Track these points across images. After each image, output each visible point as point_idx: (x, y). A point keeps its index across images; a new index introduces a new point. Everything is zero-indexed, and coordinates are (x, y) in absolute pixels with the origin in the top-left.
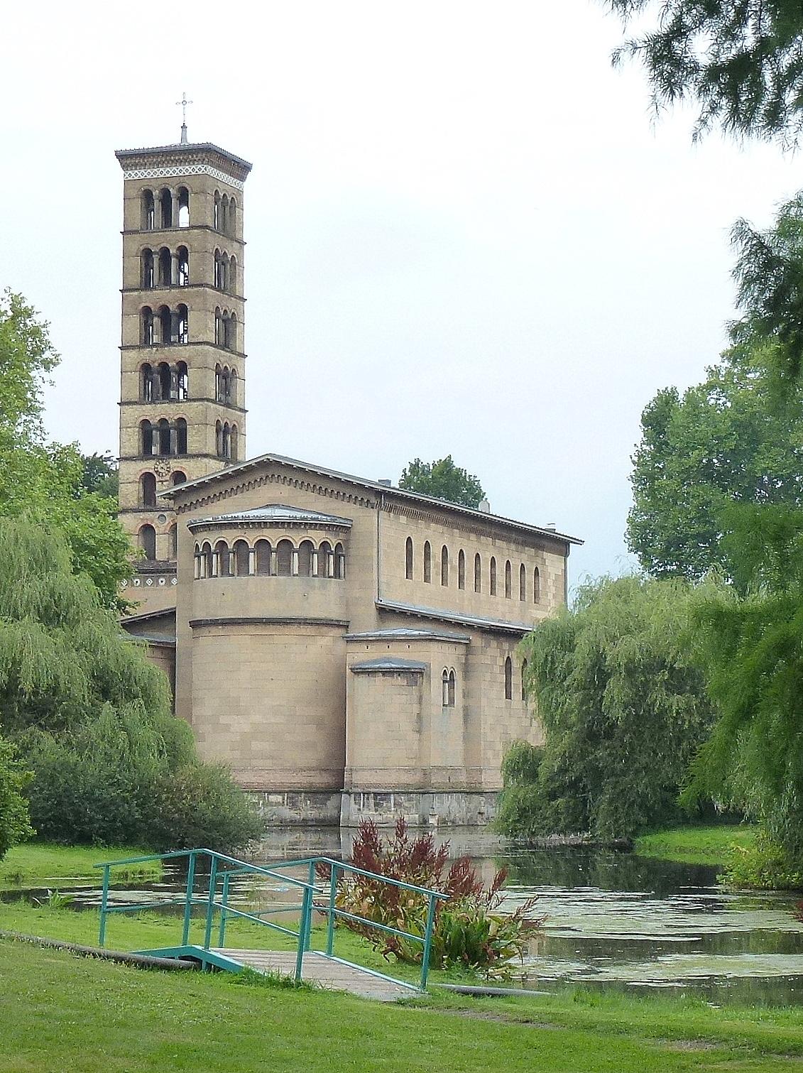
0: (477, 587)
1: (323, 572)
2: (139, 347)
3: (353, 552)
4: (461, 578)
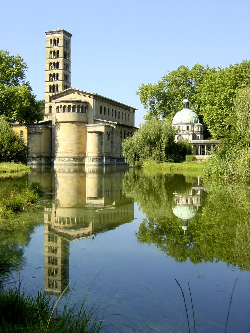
3: (89, 108)
4: (112, 115)
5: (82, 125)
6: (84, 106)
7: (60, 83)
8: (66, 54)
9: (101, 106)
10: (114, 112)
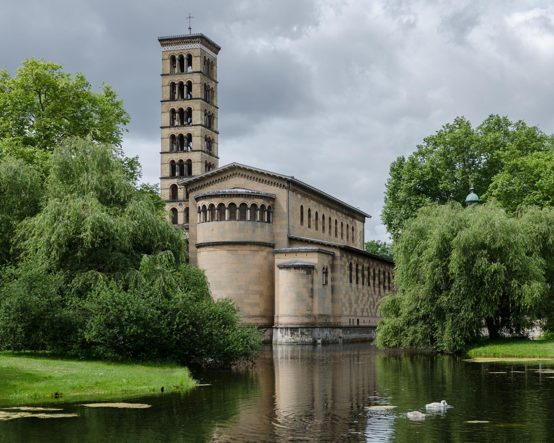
0: (330, 233)
1: (262, 220)
2: (169, 127)
3: (276, 210)
4: (323, 227)
5: (262, 251)
6: (267, 205)
7: (196, 158)
8: (208, 91)
9: (302, 207)
10: (327, 221)
